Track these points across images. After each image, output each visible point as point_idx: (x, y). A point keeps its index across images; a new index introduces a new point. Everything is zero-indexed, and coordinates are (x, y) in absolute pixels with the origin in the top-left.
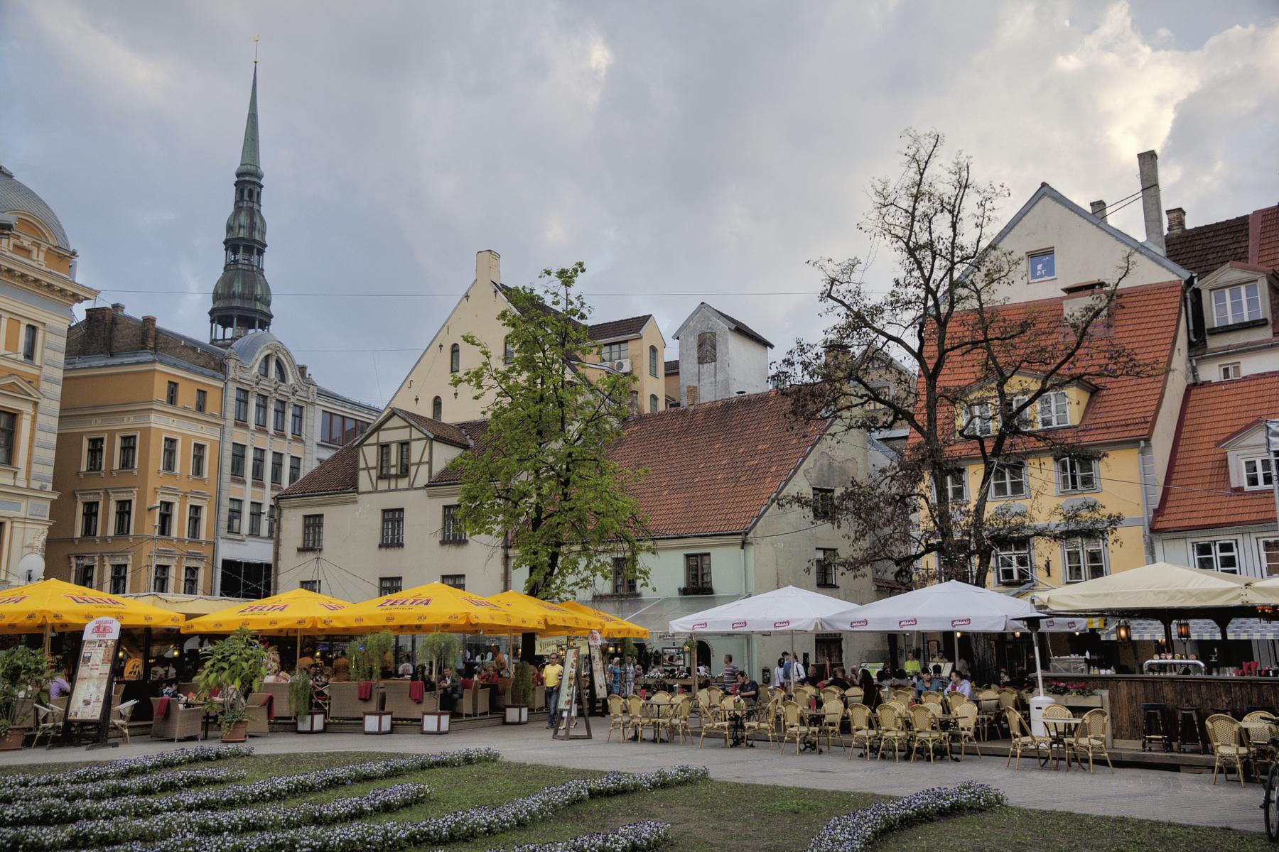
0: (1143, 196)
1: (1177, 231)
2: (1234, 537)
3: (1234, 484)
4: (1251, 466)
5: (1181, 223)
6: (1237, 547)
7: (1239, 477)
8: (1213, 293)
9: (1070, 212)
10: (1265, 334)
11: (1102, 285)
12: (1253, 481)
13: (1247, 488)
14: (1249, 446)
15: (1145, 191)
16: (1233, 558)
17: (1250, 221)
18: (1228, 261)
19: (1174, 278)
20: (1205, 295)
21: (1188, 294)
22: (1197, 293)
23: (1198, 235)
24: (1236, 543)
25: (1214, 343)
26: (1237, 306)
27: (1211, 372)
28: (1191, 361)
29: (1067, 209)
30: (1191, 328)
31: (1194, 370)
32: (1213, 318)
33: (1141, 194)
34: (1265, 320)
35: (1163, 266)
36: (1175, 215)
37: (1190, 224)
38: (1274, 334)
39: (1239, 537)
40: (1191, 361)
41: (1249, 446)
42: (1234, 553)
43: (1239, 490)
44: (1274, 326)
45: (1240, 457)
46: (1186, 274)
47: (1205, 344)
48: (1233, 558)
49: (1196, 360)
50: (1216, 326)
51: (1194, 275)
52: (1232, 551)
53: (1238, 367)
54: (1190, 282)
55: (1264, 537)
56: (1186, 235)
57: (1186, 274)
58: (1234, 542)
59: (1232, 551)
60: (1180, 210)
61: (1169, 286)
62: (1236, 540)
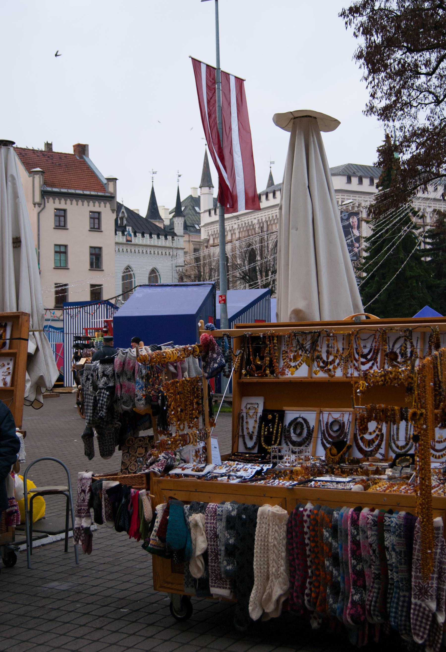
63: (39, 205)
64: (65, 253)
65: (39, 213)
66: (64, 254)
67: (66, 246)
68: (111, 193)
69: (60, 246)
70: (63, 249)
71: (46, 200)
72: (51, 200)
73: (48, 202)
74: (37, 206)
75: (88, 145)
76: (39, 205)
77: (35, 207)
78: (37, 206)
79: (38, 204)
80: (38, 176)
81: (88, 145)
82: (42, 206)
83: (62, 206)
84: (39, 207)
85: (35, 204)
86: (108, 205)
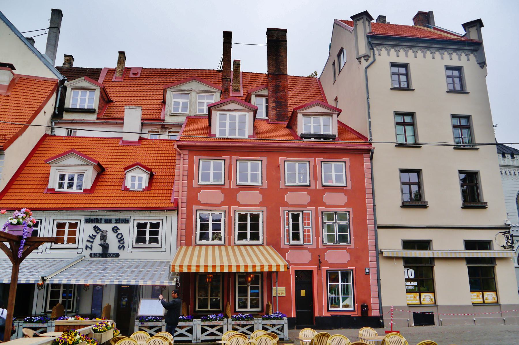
0: (49, 33)
1: (67, 66)
2: (40, 218)
3: (50, 186)
4: (62, 177)
5: (71, 64)
6: (41, 224)
7: (53, 183)
8: (73, 91)
9: (6, 25)
10: (93, 117)
11: (11, 67)
12: (61, 186)
13: (57, 190)
14: (64, 165)
15: (51, 29)
16: (38, 230)
17: (102, 71)
18: (84, 76)
19: (55, 77)
20: (69, 90)
21: (60, 89)
22: (65, 88)
23: (77, 70)
24: (41, 222)
25: (67, 117)
26: (83, 100)
27: (61, 132)
28: (52, 122)
29: (4, 24)
30: (57, 106)
31: (52, 129)
32: (69, 104)
33: (47, 31)
34: (95, 110)
35: (51, 70)
36: (68, 58)
37: (75, 65)
38: (97, 119)
39: (43, 218)
40: (52, 122)
41: (64, 165)
42: (38, 229)
43: (53, 190)
44: (98, 114)
45: (58, 171)
46: (61, 77)
47: (62, 116)
48: (38, 230)
49: (55, 123)
50: (70, 107)
51: (66, 79)
52: (37, 227)
53: (76, 132)
54: (63, 82)
55: (57, 220)
56: (71, 69)
57: (61, 77)
58: (40, 221)
59: (37, 227)
60: (71, 56)
61: (52, 80)
62: (41, 220)
63: (367, 57)
64: (413, 124)
65: (367, 68)
66: (416, 174)
67: (412, 115)
68: (476, 41)
69: (404, 114)
70: (408, 119)
71: (376, 52)
72: (384, 51)
73: (379, 55)
74: (363, 59)
75: (432, 12)
76: (367, 57)
77: (360, 62)
78: (363, 59)
79: (364, 57)
80: (362, 20)
81: (432, 12)
82: (371, 60)
83: (402, 59)
84: (367, 60)
85: (359, 59)
86: (472, 57)
